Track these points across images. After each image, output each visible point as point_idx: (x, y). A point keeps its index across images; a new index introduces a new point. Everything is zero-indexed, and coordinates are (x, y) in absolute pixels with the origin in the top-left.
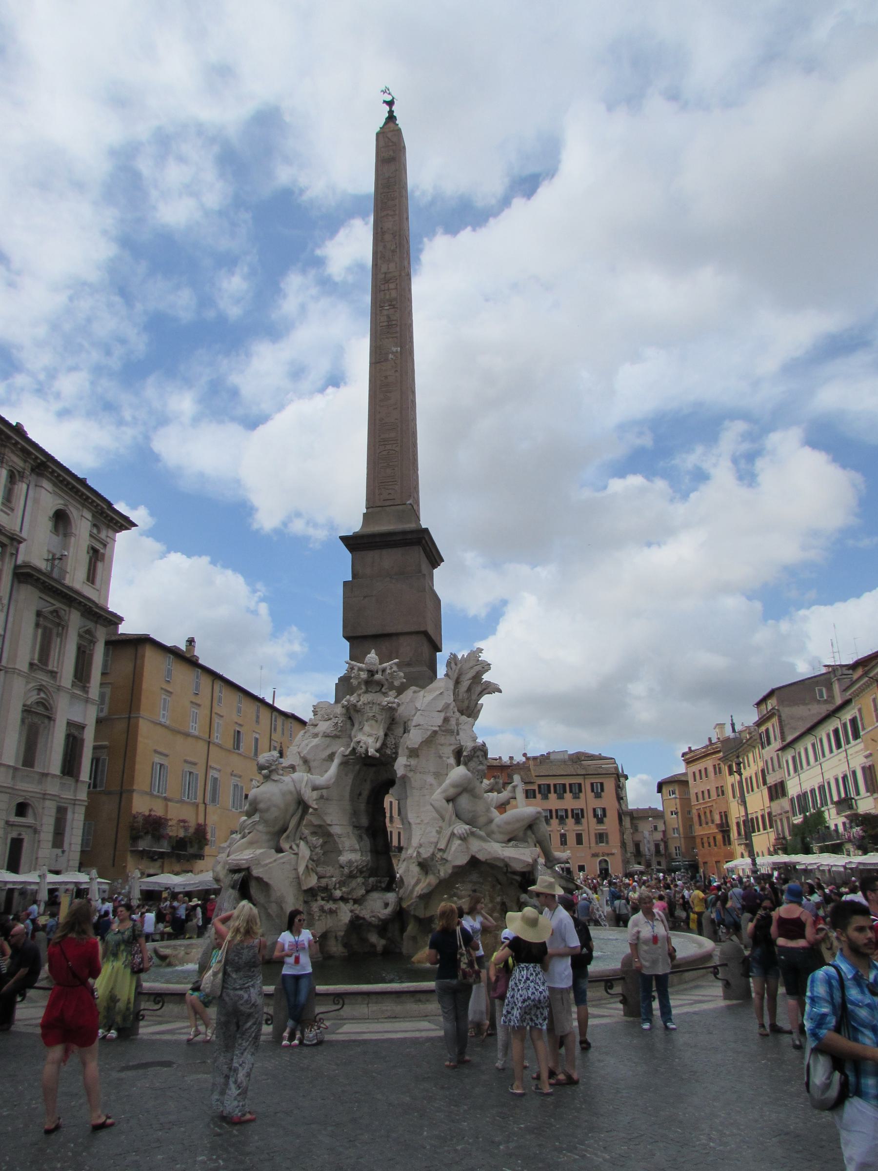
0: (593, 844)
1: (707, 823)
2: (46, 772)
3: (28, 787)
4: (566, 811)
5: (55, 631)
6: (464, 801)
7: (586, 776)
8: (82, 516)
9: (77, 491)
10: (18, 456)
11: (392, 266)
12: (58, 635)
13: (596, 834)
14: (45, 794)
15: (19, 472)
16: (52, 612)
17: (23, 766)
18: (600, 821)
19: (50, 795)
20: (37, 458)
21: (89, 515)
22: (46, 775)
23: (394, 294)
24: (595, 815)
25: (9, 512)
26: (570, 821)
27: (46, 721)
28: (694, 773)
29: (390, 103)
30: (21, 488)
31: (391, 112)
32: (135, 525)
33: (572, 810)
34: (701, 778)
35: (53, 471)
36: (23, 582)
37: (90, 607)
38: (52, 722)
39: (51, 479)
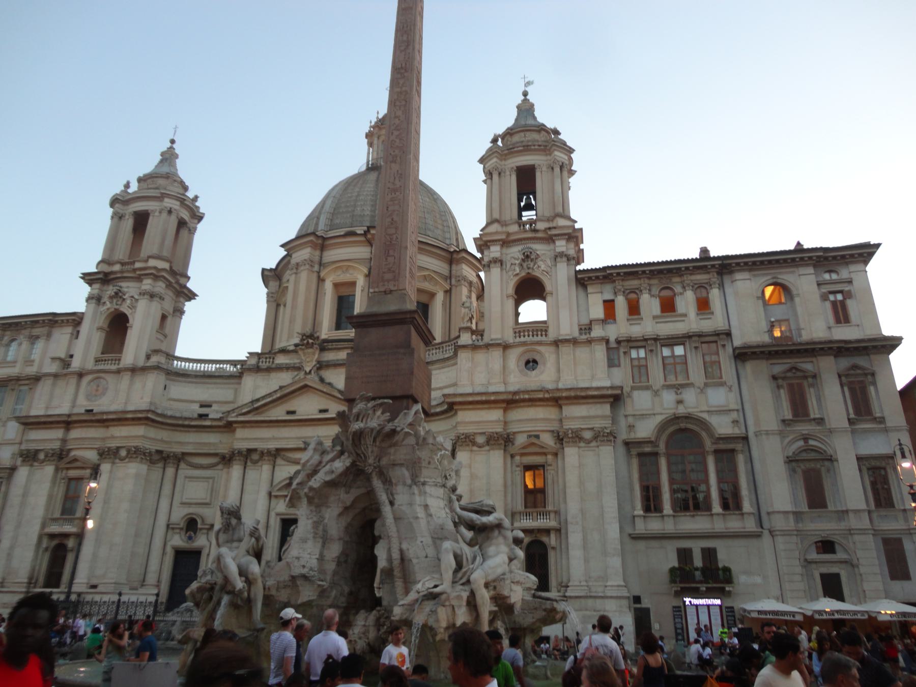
2: (844, 509)
3: (823, 526)
5: (805, 384)
8: (799, 275)
9: (777, 261)
10: (698, 274)
12: (811, 385)
14: (850, 530)
15: (707, 283)
16: (790, 370)
17: (810, 507)
19: (856, 529)
20: (713, 266)
21: (811, 270)
22: (847, 511)
25: (709, 316)
27: (827, 463)
30: (715, 294)
32: (877, 246)
35: (738, 264)
36: (746, 361)
37: (838, 348)
38: (835, 463)
39: (744, 269)
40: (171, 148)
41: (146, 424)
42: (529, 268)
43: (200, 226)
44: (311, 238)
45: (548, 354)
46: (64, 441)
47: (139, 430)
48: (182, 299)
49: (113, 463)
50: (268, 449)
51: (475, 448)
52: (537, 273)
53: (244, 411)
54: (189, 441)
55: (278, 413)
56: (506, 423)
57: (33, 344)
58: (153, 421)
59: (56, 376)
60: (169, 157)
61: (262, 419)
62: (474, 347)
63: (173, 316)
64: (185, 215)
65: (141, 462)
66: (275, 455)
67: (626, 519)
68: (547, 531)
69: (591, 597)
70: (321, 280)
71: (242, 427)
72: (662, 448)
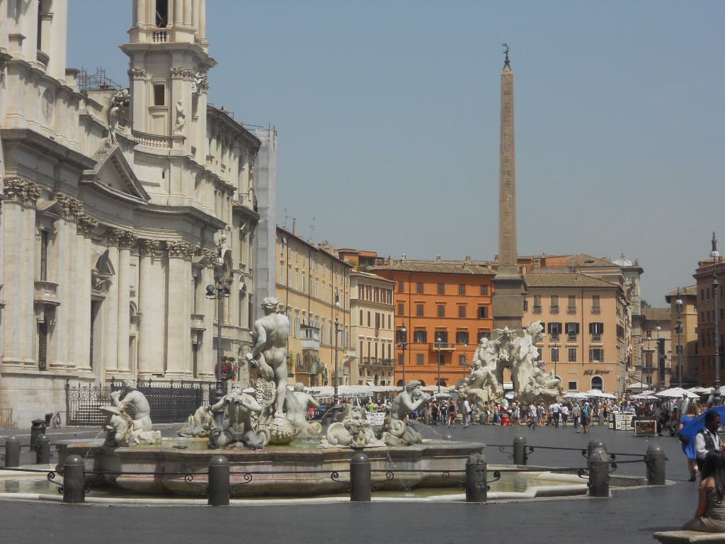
0: (587, 360)
1: (709, 345)
4: (560, 325)
6: (539, 378)
7: (585, 289)
11: (509, 153)
13: (590, 351)
18: (597, 339)
23: (509, 169)
24: (591, 331)
26: (563, 337)
28: (703, 291)
29: (507, 53)
31: (507, 57)
33: (567, 325)
34: (708, 298)
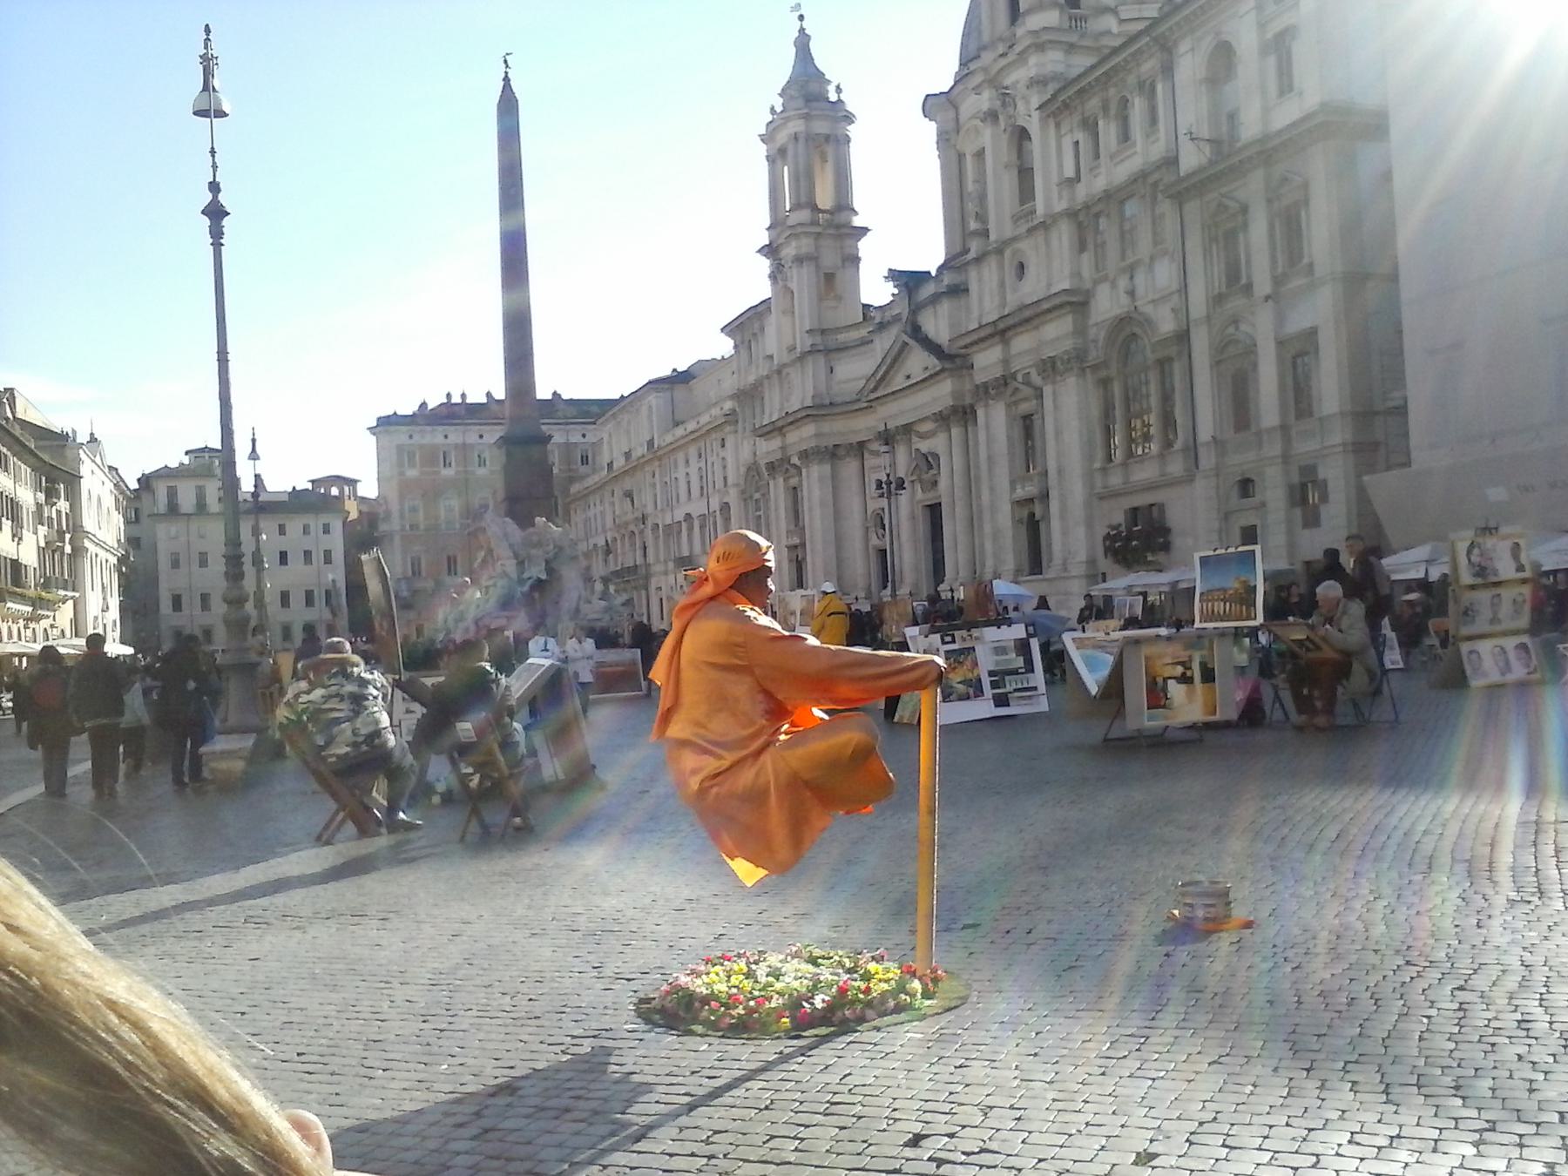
40: (802, 30)
41: (813, 421)
42: (1010, 117)
43: (853, 130)
44: (930, 100)
45: (1029, 249)
46: (783, 448)
47: (809, 430)
48: (848, 242)
49: (807, 467)
50: (897, 427)
51: (991, 402)
52: (1020, 122)
53: (872, 387)
54: (864, 426)
55: (898, 382)
56: (1006, 362)
57: (758, 342)
58: (817, 415)
59: (768, 377)
60: (803, 43)
61: (890, 391)
62: (978, 260)
63: (843, 266)
64: (821, 127)
65: (821, 462)
66: (907, 429)
67: (1089, 475)
68: (1031, 500)
69: (1064, 578)
70: (961, 157)
71: (882, 405)
72: (1113, 371)
